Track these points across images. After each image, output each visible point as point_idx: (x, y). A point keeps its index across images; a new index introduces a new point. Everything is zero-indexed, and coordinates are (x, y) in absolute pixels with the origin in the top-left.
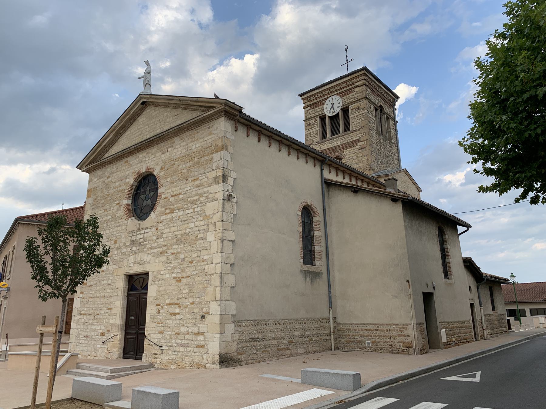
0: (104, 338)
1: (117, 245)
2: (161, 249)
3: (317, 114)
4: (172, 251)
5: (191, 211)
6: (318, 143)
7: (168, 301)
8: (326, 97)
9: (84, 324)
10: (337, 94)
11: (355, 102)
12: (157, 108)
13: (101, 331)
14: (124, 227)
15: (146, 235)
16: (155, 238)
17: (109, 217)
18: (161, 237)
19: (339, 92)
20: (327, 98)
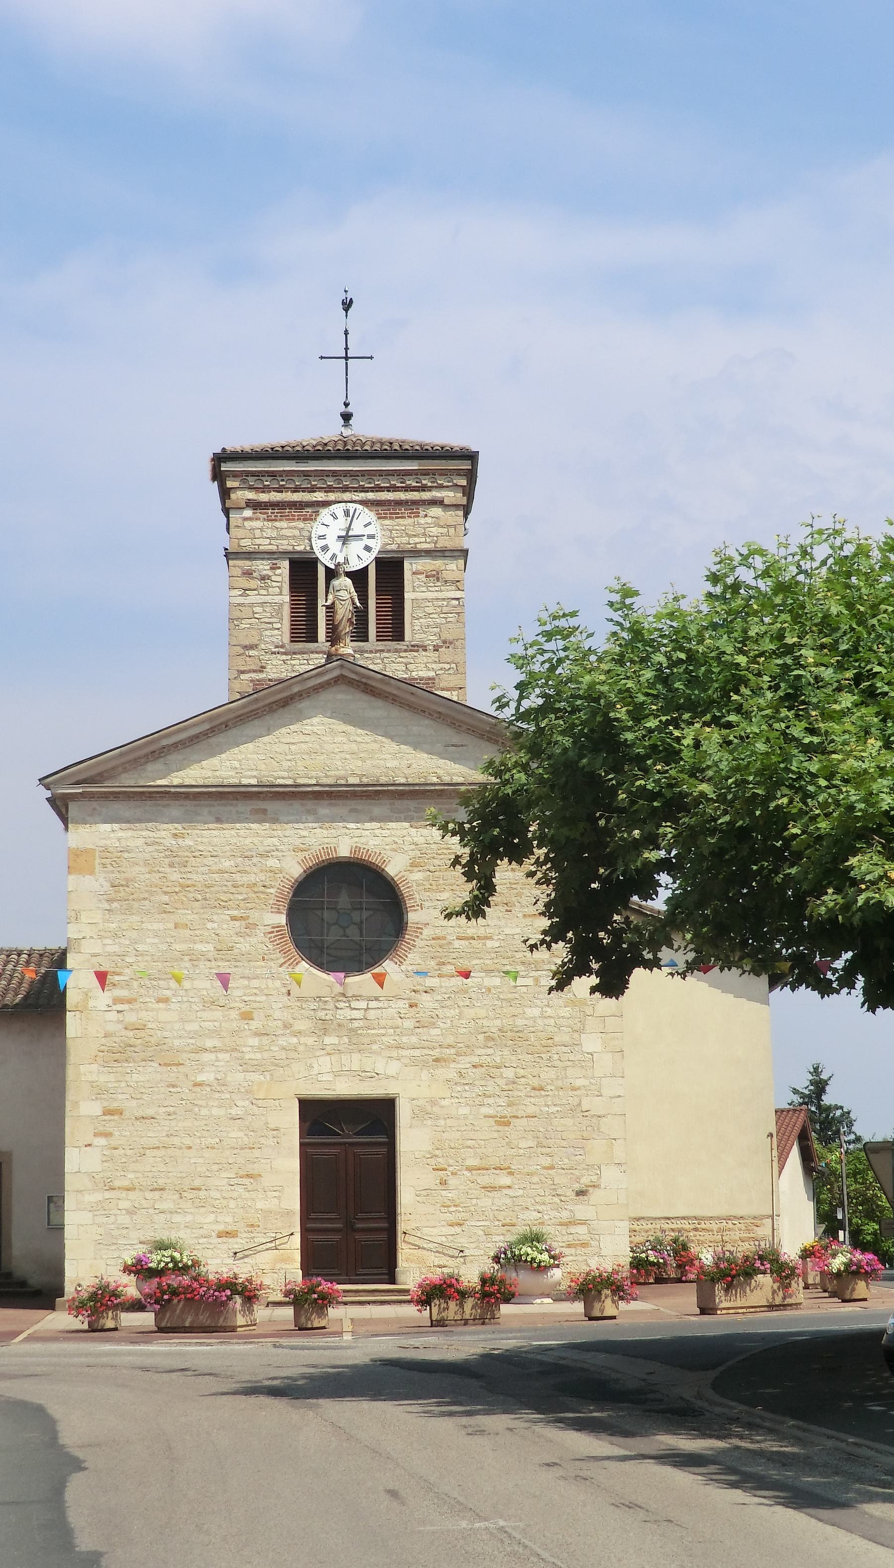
0: (236, 1244)
1: (254, 1025)
2: (436, 1053)
3: (285, 545)
4: (476, 1060)
5: (530, 981)
6: (279, 650)
7: (471, 1162)
8: (319, 496)
9: (130, 1212)
10: (363, 503)
11: (428, 553)
12: (379, 703)
13: (221, 1227)
14: (278, 983)
15: (372, 1014)
16: (409, 1024)
17: (199, 946)
18: (433, 1025)
19: (371, 496)
20: (326, 504)
